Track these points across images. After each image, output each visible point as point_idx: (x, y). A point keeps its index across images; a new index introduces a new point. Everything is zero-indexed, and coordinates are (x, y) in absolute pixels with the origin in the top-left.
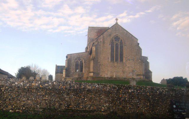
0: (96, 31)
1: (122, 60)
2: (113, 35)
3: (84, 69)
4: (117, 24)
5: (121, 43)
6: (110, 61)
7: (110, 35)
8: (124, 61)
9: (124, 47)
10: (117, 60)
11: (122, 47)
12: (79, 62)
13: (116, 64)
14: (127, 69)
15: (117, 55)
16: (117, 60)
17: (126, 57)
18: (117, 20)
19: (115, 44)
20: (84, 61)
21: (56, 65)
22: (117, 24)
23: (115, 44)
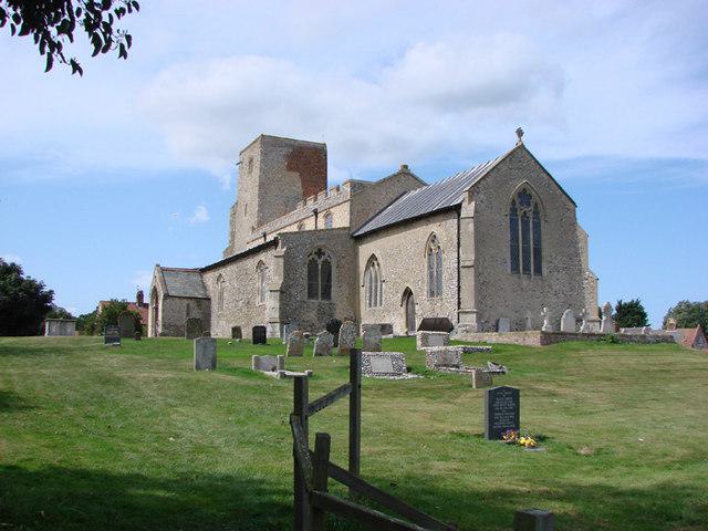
0: (285, 151)
1: (538, 270)
4: (521, 148)
5: (536, 213)
6: (509, 270)
8: (545, 270)
9: (544, 227)
10: (527, 269)
11: (537, 226)
12: (320, 262)
13: (525, 283)
16: (527, 269)
17: (549, 259)
18: (520, 133)
19: (520, 213)
20: (334, 263)
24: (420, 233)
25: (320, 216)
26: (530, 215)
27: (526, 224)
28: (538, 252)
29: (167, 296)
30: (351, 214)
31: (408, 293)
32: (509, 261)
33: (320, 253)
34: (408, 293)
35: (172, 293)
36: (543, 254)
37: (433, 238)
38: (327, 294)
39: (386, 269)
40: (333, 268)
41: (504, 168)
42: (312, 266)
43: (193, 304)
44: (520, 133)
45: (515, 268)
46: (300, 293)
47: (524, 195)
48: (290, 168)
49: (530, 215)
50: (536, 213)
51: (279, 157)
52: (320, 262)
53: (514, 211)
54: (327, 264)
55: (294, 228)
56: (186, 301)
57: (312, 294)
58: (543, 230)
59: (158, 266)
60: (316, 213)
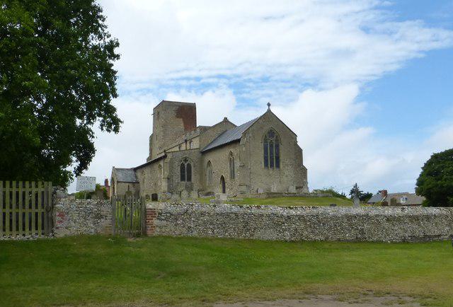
1: (278, 166)
2: (267, 128)
3: (193, 177)
4: (269, 111)
7: (262, 128)
8: (281, 166)
9: (281, 147)
10: (272, 166)
11: (277, 146)
14: (285, 179)
15: (272, 158)
16: (272, 166)
18: (269, 105)
19: (269, 141)
21: (114, 167)
22: (269, 111)
23: (269, 141)
24: (226, 152)
25: (188, 142)
26: (274, 142)
27: (271, 146)
28: (278, 158)
29: (118, 182)
30: (200, 141)
31: (222, 178)
32: (263, 163)
33: (186, 160)
34: (222, 178)
35: (122, 180)
36: (281, 158)
37: (231, 154)
38: (189, 179)
39: (215, 168)
40: (192, 167)
41: (261, 121)
42: (182, 166)
43: (131, 185)
44: (269, 105)
45: (266, 165)
46: (177, 178)
47: (271, 133)
48: (177, 117)
49: (274, 142)
50: (277, 140)
51: (172, 112)
52: (186, 165)
53: (265, 141)
54: (189, 165)
55: (177, 149)
56: (127, 184)
57: (183, 179)
58: (280, 148)
59: (114, 167)
60: (186, 141)
